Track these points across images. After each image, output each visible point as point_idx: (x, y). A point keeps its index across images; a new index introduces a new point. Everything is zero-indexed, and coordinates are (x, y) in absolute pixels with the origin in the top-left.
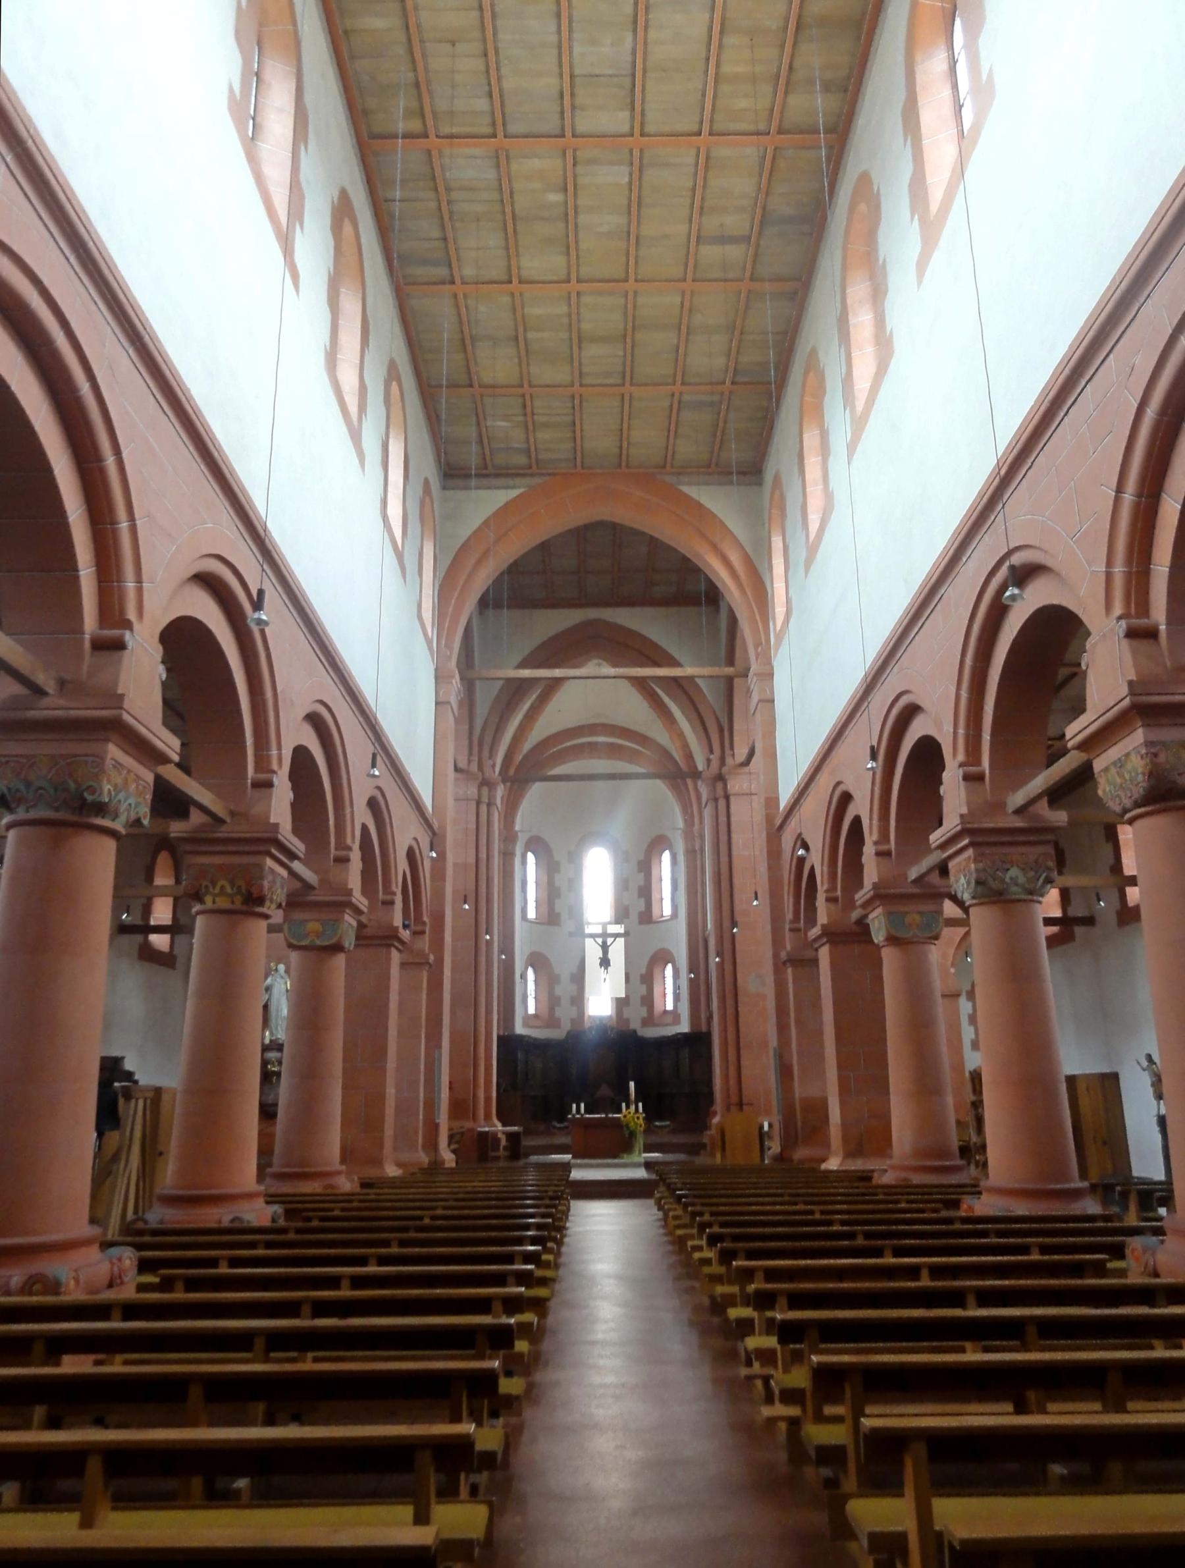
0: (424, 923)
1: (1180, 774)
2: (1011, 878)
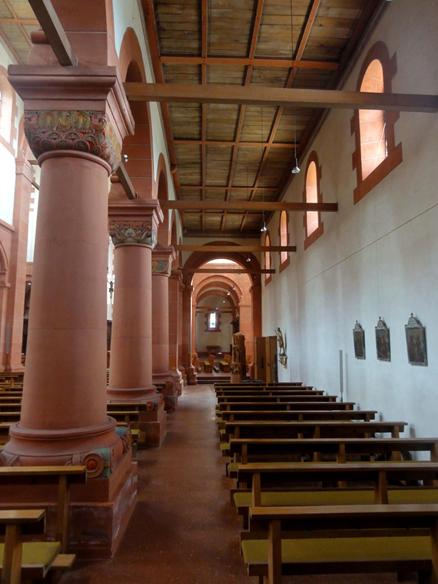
0: (6, 270)
1: (44, 133)
2: (128, 234)
